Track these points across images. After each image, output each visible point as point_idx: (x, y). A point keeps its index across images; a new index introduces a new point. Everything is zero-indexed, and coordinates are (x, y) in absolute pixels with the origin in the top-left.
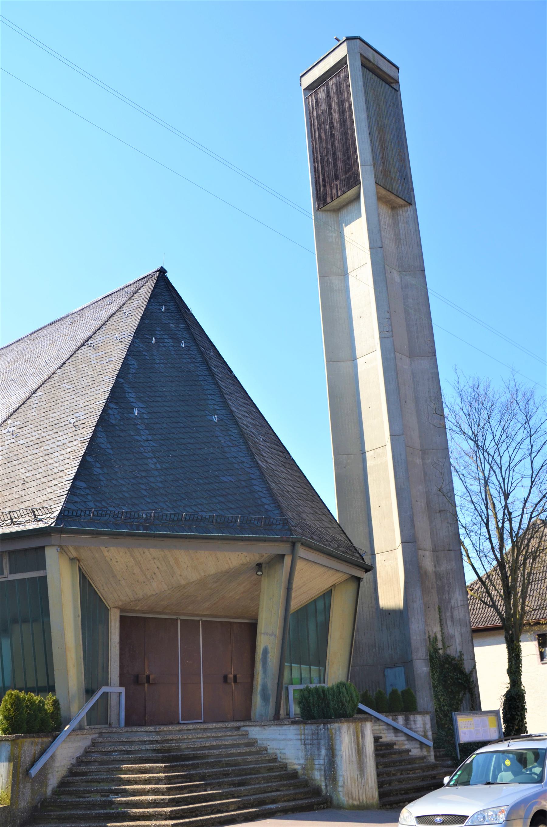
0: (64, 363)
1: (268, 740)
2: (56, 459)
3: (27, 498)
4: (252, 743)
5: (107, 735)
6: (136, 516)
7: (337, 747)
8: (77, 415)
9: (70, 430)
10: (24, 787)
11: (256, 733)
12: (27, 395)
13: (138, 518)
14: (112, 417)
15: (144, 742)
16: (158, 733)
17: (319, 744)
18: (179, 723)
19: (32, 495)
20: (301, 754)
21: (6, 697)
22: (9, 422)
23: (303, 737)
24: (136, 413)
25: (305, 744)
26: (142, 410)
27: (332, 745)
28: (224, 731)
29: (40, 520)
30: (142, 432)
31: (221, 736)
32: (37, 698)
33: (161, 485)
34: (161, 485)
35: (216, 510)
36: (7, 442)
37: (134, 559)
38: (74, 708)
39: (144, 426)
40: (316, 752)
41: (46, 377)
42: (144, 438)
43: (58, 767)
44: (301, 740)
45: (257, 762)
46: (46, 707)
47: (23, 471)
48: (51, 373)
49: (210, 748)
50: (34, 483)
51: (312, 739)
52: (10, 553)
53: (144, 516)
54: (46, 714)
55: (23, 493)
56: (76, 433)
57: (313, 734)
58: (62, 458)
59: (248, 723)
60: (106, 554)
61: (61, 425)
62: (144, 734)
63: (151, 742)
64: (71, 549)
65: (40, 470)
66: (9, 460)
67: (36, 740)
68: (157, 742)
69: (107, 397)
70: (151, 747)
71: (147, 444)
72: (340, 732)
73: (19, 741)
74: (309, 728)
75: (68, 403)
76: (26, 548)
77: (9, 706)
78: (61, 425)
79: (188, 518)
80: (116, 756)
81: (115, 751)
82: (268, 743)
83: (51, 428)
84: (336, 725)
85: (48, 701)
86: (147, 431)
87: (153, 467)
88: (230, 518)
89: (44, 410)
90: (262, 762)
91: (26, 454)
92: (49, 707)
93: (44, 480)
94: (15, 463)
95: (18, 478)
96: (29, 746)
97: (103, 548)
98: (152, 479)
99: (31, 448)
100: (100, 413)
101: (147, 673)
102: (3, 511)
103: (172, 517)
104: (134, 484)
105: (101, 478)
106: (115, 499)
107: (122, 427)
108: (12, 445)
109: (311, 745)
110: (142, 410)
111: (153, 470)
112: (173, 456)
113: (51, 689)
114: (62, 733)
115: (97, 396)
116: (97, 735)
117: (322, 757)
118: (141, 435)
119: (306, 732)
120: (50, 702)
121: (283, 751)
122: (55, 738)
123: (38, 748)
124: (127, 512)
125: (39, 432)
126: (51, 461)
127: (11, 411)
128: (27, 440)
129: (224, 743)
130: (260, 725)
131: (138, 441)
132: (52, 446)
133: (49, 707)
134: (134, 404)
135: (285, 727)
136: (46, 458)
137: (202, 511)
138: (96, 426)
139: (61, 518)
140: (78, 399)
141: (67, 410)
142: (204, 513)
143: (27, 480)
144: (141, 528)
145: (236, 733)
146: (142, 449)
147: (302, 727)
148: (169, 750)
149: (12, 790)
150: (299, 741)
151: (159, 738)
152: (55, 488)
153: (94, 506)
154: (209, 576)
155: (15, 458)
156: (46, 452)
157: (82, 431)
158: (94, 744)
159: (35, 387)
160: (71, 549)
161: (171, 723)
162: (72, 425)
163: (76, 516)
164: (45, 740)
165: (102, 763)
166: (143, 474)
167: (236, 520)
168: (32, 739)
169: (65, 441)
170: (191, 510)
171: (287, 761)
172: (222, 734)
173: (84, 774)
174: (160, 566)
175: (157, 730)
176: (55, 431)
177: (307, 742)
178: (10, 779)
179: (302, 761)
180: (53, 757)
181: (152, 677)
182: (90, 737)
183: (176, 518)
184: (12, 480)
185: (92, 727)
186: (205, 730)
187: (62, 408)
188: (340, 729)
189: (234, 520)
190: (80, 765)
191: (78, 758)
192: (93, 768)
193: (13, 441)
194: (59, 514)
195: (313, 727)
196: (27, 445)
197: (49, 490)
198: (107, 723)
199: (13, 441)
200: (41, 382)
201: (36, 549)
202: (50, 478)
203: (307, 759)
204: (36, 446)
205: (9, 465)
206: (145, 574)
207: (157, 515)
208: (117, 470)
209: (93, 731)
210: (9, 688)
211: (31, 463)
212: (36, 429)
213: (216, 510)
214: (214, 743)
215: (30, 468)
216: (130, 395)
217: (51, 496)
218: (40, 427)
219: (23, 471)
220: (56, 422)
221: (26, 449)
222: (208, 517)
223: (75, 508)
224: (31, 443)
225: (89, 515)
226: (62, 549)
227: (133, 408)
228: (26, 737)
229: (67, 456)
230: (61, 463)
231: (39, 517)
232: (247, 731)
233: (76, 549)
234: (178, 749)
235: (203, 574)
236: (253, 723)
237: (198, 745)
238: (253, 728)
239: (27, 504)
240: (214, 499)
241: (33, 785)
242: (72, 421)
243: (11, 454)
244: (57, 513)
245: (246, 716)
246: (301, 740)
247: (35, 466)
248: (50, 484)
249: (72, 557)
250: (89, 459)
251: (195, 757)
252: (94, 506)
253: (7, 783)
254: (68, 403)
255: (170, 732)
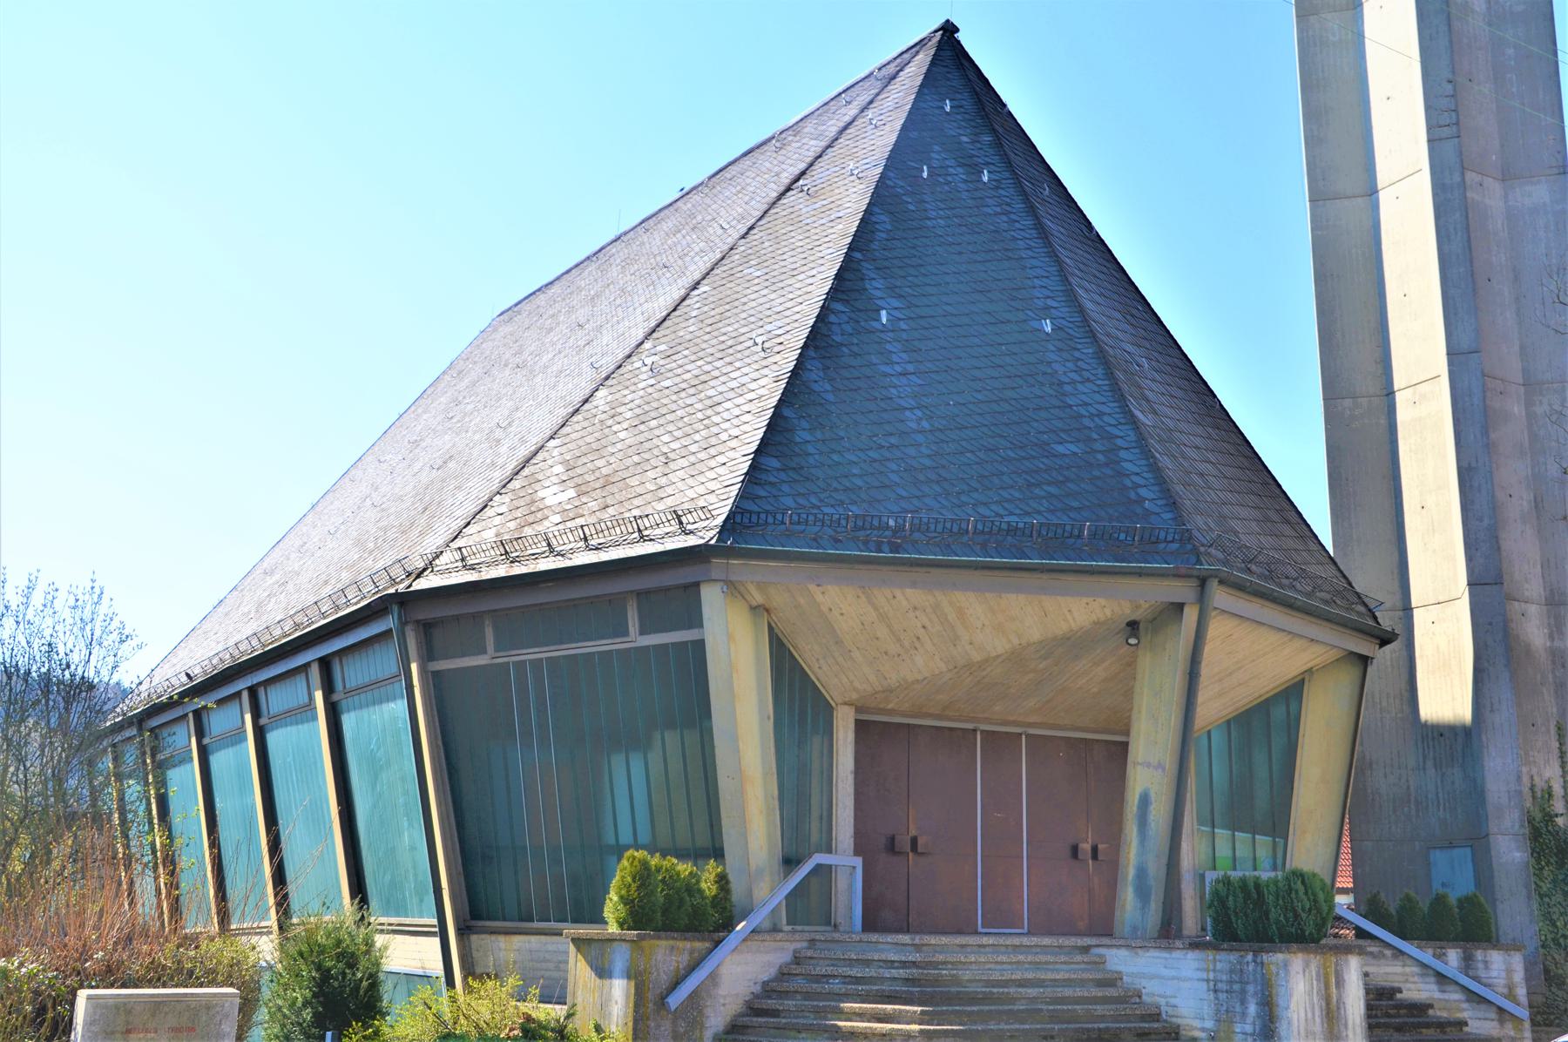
0: (751, 228)
1: (1143, 976)
2: (726, 415)
3: (669, 490)
4: (1111, 981)
5: (823, 946)
6: (876, 523)
7: (1281, 1002)
8: (769, 327)
9: (756, 358)
10: (659, 1026)
11: (1120, 960)
12: (683, 292)
13: (879, 528)
14: (834, 328)
15: (890, 964)
16: (918, 948)
17: (1243, 992)
18: (976, 933)
19: (680, 485)
20: (1207, 1010)
21: (625, 863)
22: (647, 345)
23: (1211, 976)
24: (884, 320)
25: (1215, 991)
26: (897, 314)
27: (1270, 996)
28: (1052, 954)
29: (691, 532)
30: (895, 358)
31: (1047, 963)
32: (684, 868)
33: (927, 462)
34: (927, 462)
35: (1039, 512)
36: (641, 386)
37: (876, 609)
38: (761, 891)
39: (899, 346)
40: (1238, 1008)
41: (719, 256)
42: (898, 368)
43: (725, 997)
44: (1208, 981)
45: (1116, 1019)
46: (703, 885)
47: (666, 438)
48: (726, 247)
49: (1022, 983)
50: (684, 462)
51: (1231, 982)
52: (641, 595)
53: (892, 523)
54: (704, 898)
55: (663, 481)
56: (765, 363)
57: (1231, 971)
58: (737, 412)
59: (1106, 941)
60: (819, 598)
61: (739, 348)
62: (891, 947)
63: (904, 964)
64: (752, 588)
65: (697, 437)
66: (643, 418)
67: (680, 944)
68: (914, 964)
69: (826, 289)
70: (902, 973)
71: (904, 380)
72: (1287, 972)
73: (644, 943)
74: (1225, 960)
75: (754, 304)
76: (663, 584)
77: (629, 879)
78: (739, 348)
79: (980, 527)
80: (836, 986)
81: (835, 976)
82: (1144, 982)
83: (719, 355)
84: (1280, 956)
85: (710, 871)
86: (904, 355)
87: (913, 425)
88: (1068, 528)
89: (710, 321)
90: (1127, 1018)
91: (674, 407)
92: (708, 886)
93: (702, 455)
94: (654, 423)
95: (656, 452)
96: (667, 954)
97: (812, 587)
98: (912, 451)
99: (683, 394)
100: (811, 322)
101: (913, 832)
102: (627, 515)
103: (948, 525)
104: (875, 461)
105: (811, 450)
106: (836, 490)
107: (855, 349)
108: (650, 390)
109: (1228, 993)
110: (897, 314)
111: (915, 431)
112: (957, 404)
113: (718, 854)
114: (732, 935)
115: (810, 289)
116: (805, 944)
117: (1250, 1020)
118: (893, 363)
119: (1219, 966)
120: (712, 877)
121: (1173, 1001)
122: (718, 943)
123: (684, 959)
124: (856, 516)
125: (700, 363)
126: (716, 419)
127: (653, 324)
128: (678, 380)
129: (1050, 976)
130: (1127, 946)
131: (886, 375)
132: (720, 389)
133: (708, 886)
134: (880, 303)
135: (1177, 954)
136: (709, 412)
137: (1012, 514)
138: (805, 347)
139: (728, 527)
140: (773, 296)
141: (752, 319)
142: (1013, 519)
143: (672, 456)
144: (885, 547)
145: (1079, 958)
146: (893, 391)
147: (1210, 954)
148: (936, 982)
149: (635, 1030)
150: (1204, 985)
151: (917, 957)
152: (721, 470)
153: (793, 505)
154: (1029, 645)
155: (653, 414)
156: (709, 403)
157: (777, 358)
158: (797, 960)
159: (697, 276)
160: (752, 588)
161: (960, 932)
162: (759, 348)
163: (758, 524)
164: (698, 945)
165: (808, 996)
166: (893, 440)
167: (1081, 531)
168: (671, 942)
169: (745, 380)
170: (987, 513)
171: (1179, 1021)
172: (1050, 958)
173: (774, 1013)
174: (928, 624)
175: (917, 941)
176: (728, 360)
177: (1219, 985)
178: (631, 1010)
179: (1209, 1024)
180: (713, 977)
181: (920, 842)
182: (792, 946)
183: (955, 529)
184: (646, 456)
185: (799, 928)
186: (1016, 948)
187: (744, 315)
188: (1286, 965)
189: (1076, 532)
190: (770, 997)
191: (765, 984)
192: (790, 1004)
193: (652, 381)
194: (725, 521)
195: (1234, 957)
196: (675, 389)
197: (711, 475)
198: (829, 923)
199: (652, 381)
200: (709, 265)
201: (686, 587)
202: (713, 451)
203: (1218, 1021)
204: (692, 391)
205: (642, 427)
206: (899, 640)
207: (917, 521)
208: (842, 434)
209: (797, 936)
210: (627, 848)
211: (680, 424)
212: (693, 358)
213: (1039, 512)
214: (1030, 975)
215: (678, 434)
216: (875, 284)
217: (712, 486)
218: (701, 354)
219: (666, 438)
220: (730, 343)
221: (674, 398)
222: (1021, 525)
223: (756, 508)
224: (684, 385)
225: (783, 523)
226: (733, 588)
227: (878, 311)
228: (659, 938)
229: (746, 408)
230: (735, 422)
231: (689, 527)
232: (1101, 956)
233: (761, 586)
234: (956, 981)
235: (1016, 641)
236: (1114, 942)
237: (996, 976)
238: (1114, 951)
239: (669, 502)
240: (1037, 491)
241: (674, 1022)
242: (759, 340)
243: (646, 408)
244: (723, 517)
245: (1103, 927)
246: (1208, 981)
247: (688, 430)
248: (713, 463)
249: (754, 604)
250: (787, 412)
251: (987, 999)
252: (793, 505)
253: (626, 1016)
254: (754, 304)
255: (943, 949)
